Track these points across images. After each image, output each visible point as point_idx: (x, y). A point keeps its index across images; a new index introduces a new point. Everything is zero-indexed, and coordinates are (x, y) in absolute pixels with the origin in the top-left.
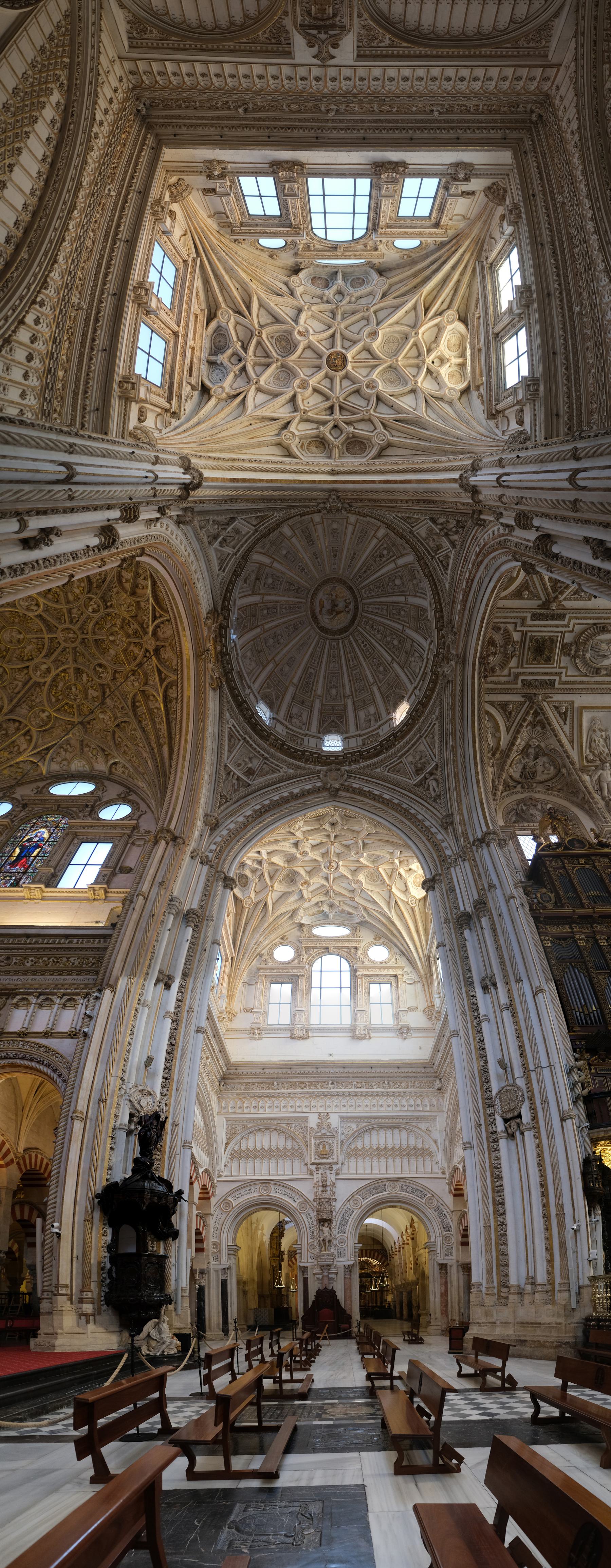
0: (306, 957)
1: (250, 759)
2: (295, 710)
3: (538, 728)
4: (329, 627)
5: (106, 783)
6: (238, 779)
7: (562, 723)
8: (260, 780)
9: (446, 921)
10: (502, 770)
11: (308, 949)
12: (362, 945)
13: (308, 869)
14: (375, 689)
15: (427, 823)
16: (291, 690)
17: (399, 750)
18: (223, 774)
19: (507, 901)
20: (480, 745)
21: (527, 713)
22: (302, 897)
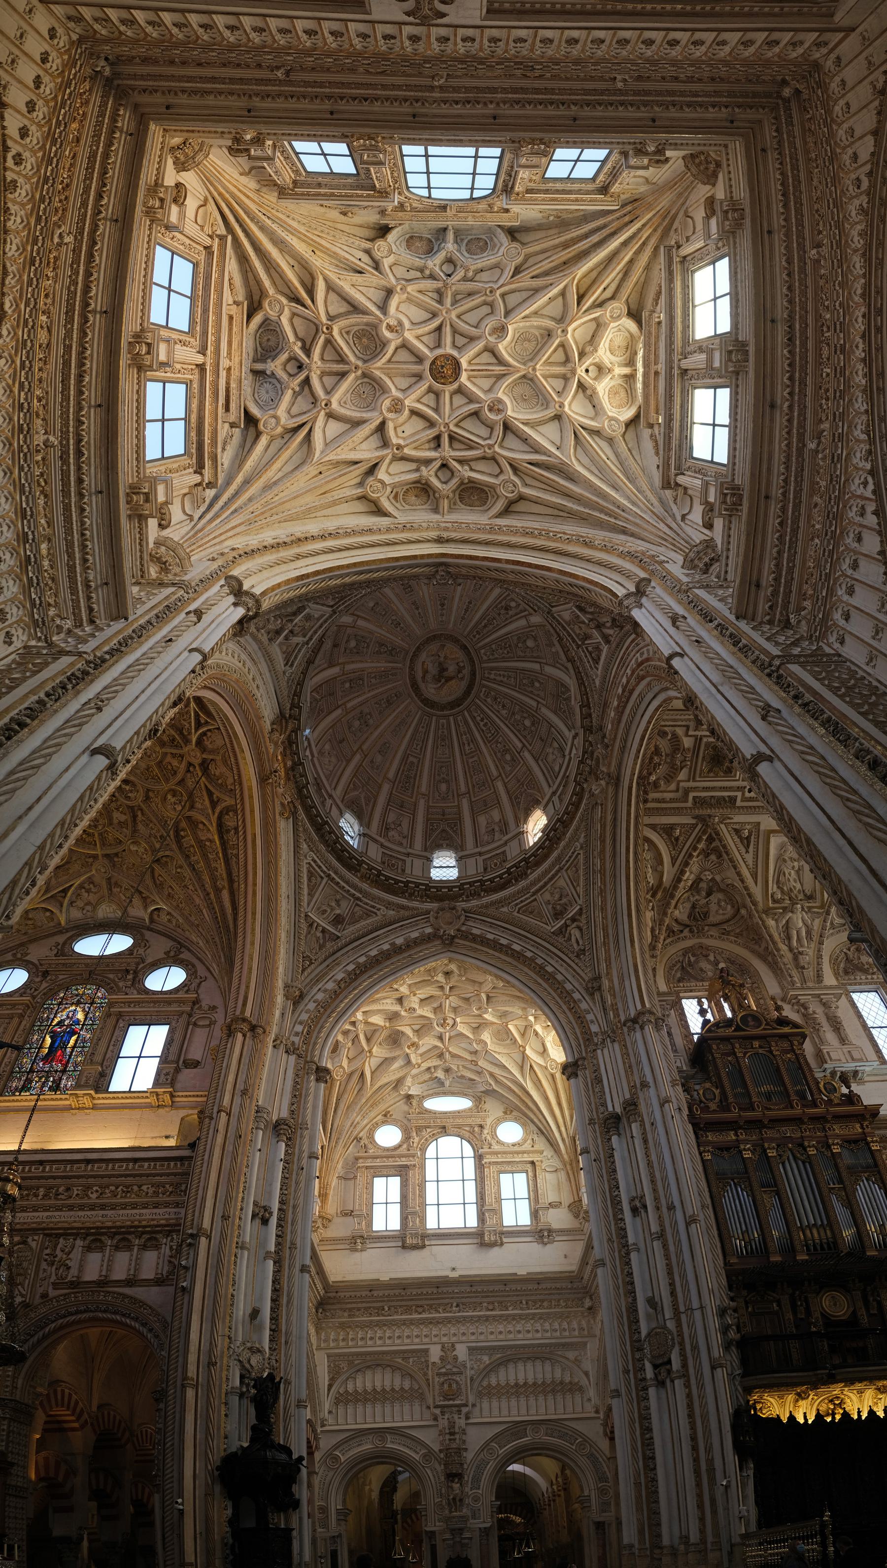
0: (416, 1140)
1: (338, 902)
2: (392, 817)
3: (713, 857)
4: (436, 699)
5: (148, 934)
6: (324, 931)
7: (743, 850)
8: (352, 928)
9: (591, 1122)
10: (665, 914)
11: (419, 1129)
12: (489, 1121)
13: (416, 1027)
14: (499, 785)
15: (568, 986)
16: (386, 788)
17: (533, 884)
18: (304, 926)
19: (662, 1106)
20: (636, 890)
21: (699, 840)
22: (409, 1062)
